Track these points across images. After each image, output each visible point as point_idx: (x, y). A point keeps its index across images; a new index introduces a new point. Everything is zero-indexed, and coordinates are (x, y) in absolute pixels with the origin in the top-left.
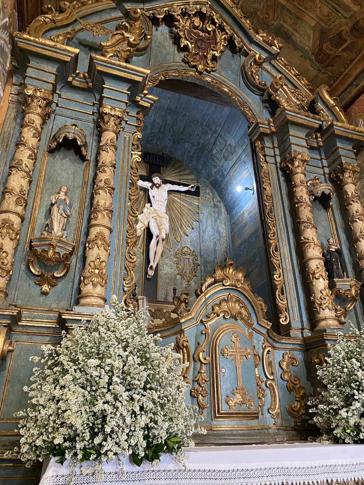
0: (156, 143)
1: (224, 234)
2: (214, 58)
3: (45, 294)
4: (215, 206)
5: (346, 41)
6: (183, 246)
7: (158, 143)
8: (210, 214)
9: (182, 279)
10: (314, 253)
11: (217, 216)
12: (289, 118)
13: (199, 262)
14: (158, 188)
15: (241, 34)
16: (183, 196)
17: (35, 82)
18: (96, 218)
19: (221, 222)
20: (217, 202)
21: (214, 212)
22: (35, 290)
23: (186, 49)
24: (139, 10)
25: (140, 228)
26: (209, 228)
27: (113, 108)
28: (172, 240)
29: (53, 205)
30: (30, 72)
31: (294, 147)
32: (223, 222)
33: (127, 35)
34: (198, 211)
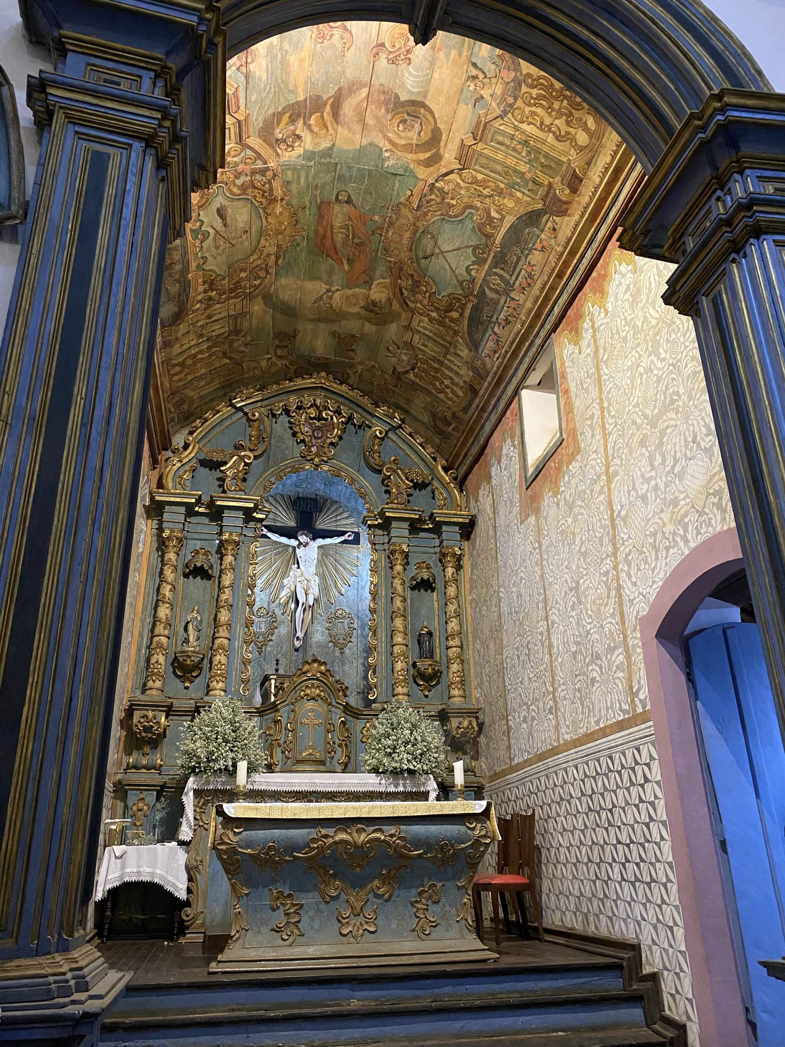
2: (332, 444)
3: (187, 688)
5: (451, 424)
10: (399, 639)
12: (387, 514)
14: (305, 546)
15: (360, 410)
17: (171, 525)
18: (218, 632)
22: (180, 685)
23: (303, 441)
24: (257, 414)
25: (284, 594)
27: (231, 534)
29: (188, 623)
30: (166, 516)
31: (393, 540)
33: (242, 454)
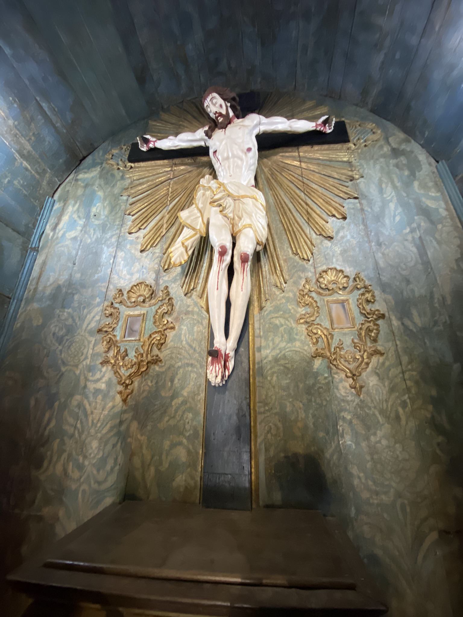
0: (230, 68)
1: (444, 213)
4: (396, 153)
6: (320, 269)
7: (233, 65)
8: (389, 174)
9: (329, 368)
11: (406, 173)
13: (380, 306)
16: (305, 152)
19: (424, 186)
20: (400, 144)
21: (397, 166)
26: (392, 206)
28: (285, 261)
32: (431, 184)
34: (350, 173)
